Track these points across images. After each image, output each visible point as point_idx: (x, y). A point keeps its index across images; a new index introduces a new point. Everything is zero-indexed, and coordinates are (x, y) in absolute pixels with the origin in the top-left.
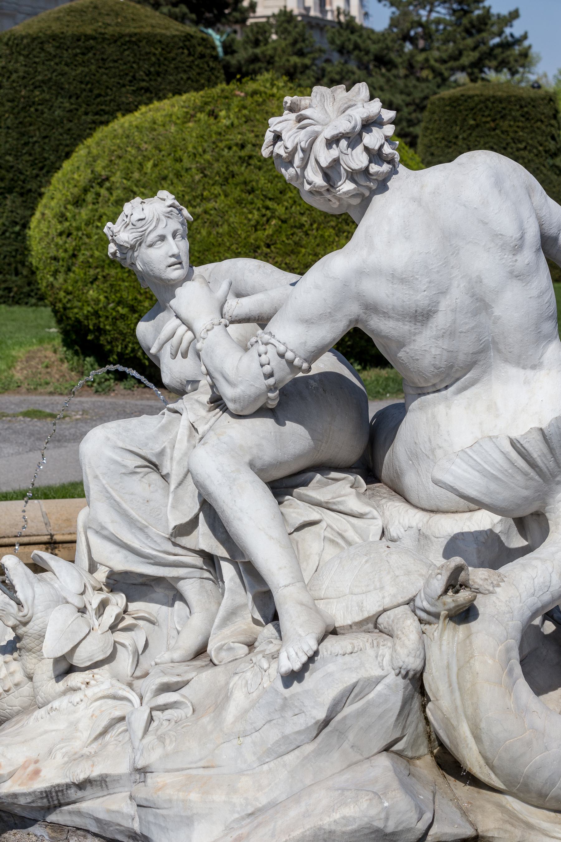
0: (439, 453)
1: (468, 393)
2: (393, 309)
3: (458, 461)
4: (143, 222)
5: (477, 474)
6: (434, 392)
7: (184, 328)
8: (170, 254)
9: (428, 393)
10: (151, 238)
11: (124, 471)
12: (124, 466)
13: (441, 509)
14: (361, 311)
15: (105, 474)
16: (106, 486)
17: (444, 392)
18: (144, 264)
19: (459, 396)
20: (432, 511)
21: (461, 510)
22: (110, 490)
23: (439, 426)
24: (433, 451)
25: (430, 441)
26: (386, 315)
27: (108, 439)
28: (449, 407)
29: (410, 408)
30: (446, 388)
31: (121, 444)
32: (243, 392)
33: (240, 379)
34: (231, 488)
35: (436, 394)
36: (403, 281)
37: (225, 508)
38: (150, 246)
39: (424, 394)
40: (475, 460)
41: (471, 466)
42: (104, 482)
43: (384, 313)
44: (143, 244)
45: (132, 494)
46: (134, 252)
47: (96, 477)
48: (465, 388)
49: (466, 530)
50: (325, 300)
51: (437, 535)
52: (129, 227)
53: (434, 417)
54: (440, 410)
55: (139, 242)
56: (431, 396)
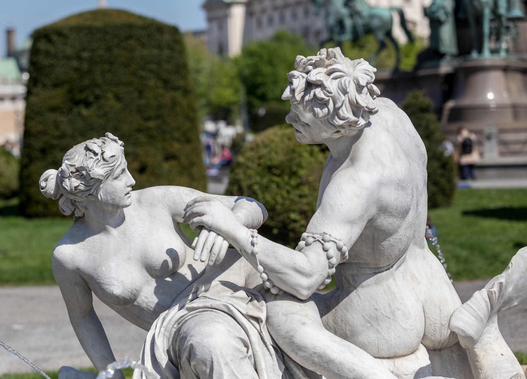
0: (398, 313)
1: (401, 268)
2: (396, 209)
3: (464, 311)
4: (114, 158)
5: (474, 318)
6: (386, 270)
7: (220, 238)
8: (129, 184)
9: (383, 272)
10: (118, 171)
11: (241, 356)
12: (242, 352)
13: (397, 355)
14: (376, 212)
15: (232, 360)
16: (234, 370)
17: (391, 270)
18: (107, 193)
19: (397, 271)
20: (389, 358)
21: (409, 353)
22: (236, 373)
23: (394, 294)
24: (393, 313)
25: (390, 306)
26: (391, 214)
27: (230, 331)
28: (394, 279)
29: (364, 283)
30: (392, 267)
31: (237, 335)
32: (317, 280)
33: (314, 270)
34: (352, 353)
35: (388, 271)
36: (403, 188)
37: (356, 368)
38: (116, 178)
39: (379, 272)
40: (474, 309)
41: (471, 314)
42: (232, 367)
43: (390, 212)
44: (110, 177)
45: (246, 374)
46: (101, 183)
47: (227, 364)
48: (400, 266)
49: (422, 366)
50: (363, 205)
51: (407, 373)
52: (100, 164)
53: (389, 288)
54: (391, 282)
55: (108, 176)
56: (385, 272)
